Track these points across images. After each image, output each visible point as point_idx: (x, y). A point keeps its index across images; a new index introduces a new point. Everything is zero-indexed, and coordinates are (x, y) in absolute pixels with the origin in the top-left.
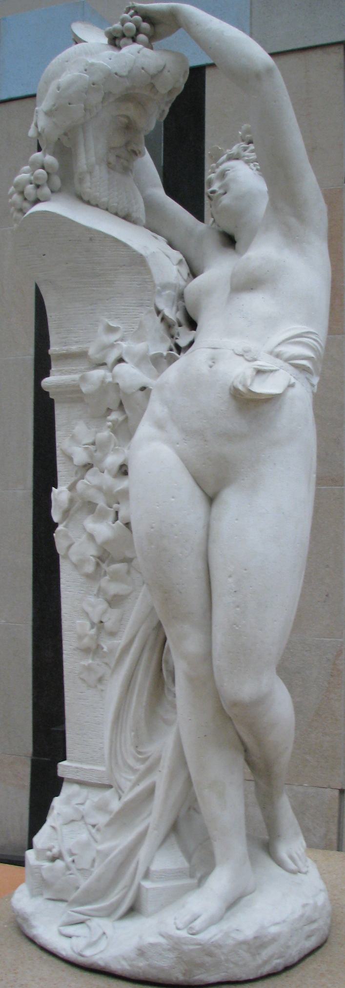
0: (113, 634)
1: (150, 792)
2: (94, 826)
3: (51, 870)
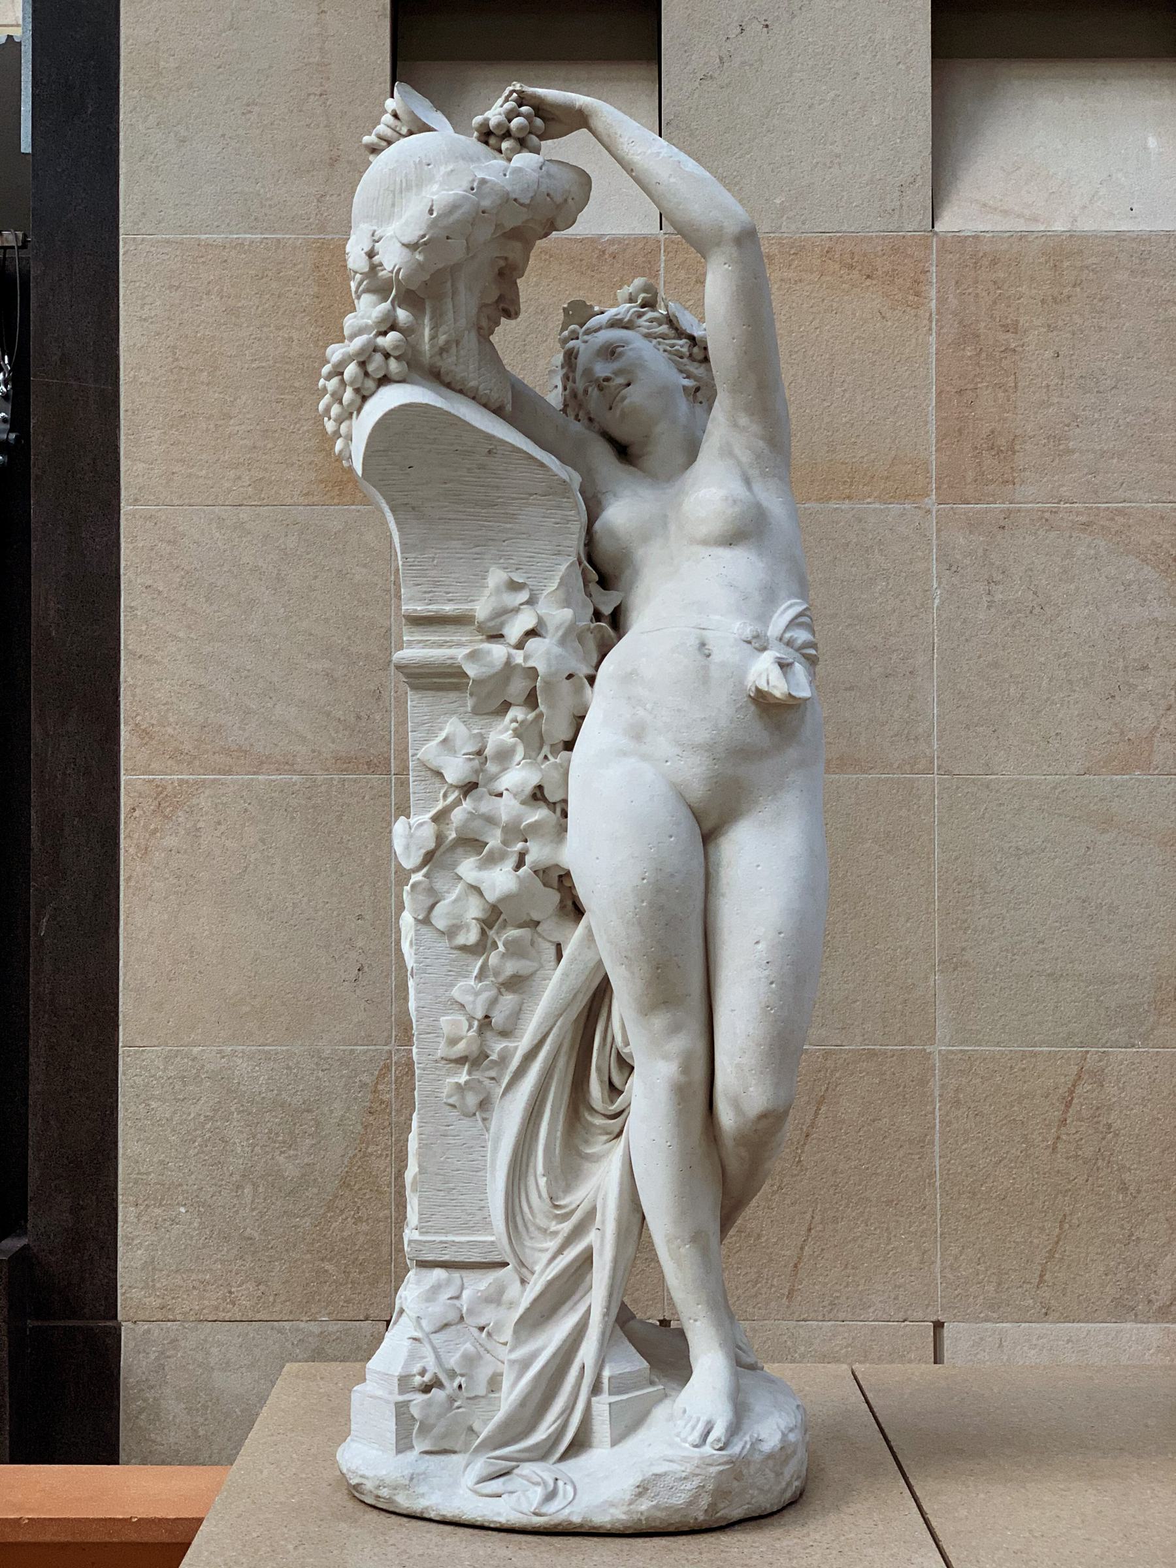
0: (505, 1034)
1: (586, 1261)
2: (482, 1329)
3: (429, 1404)
